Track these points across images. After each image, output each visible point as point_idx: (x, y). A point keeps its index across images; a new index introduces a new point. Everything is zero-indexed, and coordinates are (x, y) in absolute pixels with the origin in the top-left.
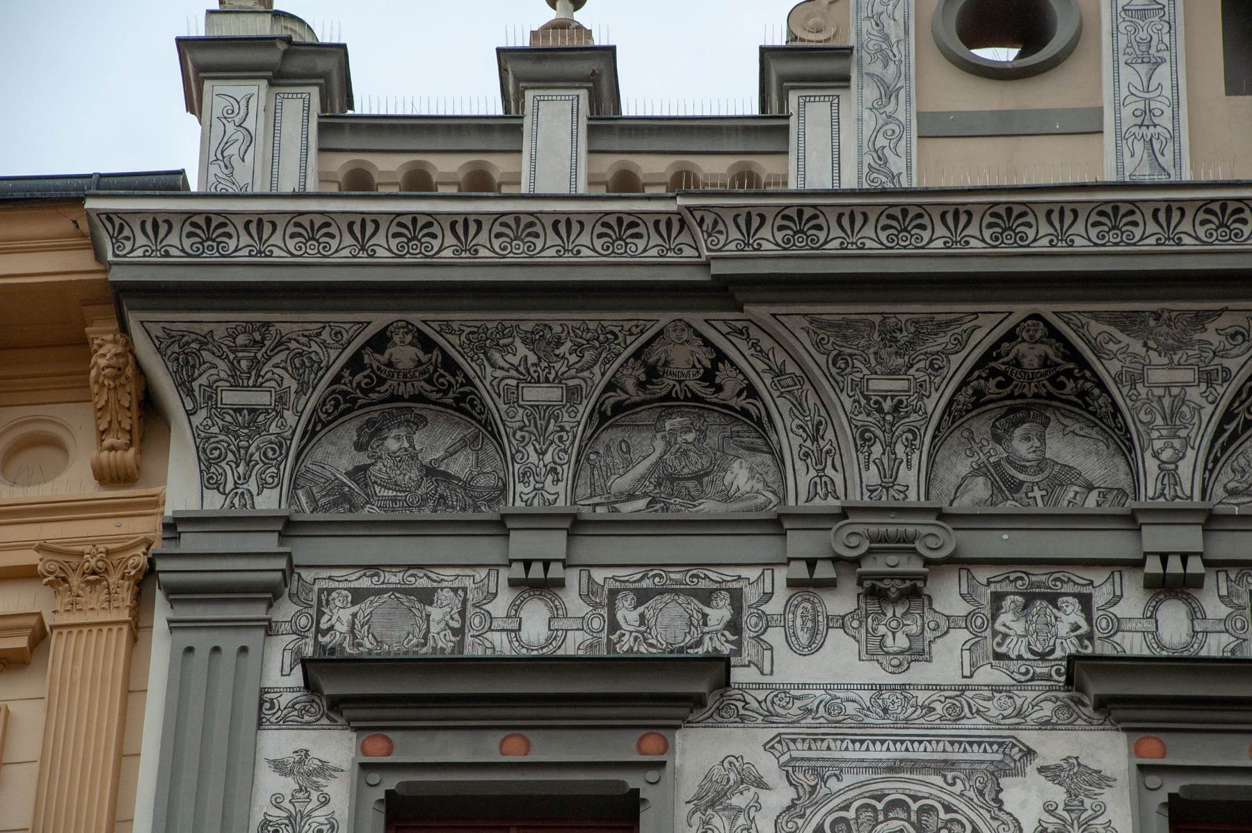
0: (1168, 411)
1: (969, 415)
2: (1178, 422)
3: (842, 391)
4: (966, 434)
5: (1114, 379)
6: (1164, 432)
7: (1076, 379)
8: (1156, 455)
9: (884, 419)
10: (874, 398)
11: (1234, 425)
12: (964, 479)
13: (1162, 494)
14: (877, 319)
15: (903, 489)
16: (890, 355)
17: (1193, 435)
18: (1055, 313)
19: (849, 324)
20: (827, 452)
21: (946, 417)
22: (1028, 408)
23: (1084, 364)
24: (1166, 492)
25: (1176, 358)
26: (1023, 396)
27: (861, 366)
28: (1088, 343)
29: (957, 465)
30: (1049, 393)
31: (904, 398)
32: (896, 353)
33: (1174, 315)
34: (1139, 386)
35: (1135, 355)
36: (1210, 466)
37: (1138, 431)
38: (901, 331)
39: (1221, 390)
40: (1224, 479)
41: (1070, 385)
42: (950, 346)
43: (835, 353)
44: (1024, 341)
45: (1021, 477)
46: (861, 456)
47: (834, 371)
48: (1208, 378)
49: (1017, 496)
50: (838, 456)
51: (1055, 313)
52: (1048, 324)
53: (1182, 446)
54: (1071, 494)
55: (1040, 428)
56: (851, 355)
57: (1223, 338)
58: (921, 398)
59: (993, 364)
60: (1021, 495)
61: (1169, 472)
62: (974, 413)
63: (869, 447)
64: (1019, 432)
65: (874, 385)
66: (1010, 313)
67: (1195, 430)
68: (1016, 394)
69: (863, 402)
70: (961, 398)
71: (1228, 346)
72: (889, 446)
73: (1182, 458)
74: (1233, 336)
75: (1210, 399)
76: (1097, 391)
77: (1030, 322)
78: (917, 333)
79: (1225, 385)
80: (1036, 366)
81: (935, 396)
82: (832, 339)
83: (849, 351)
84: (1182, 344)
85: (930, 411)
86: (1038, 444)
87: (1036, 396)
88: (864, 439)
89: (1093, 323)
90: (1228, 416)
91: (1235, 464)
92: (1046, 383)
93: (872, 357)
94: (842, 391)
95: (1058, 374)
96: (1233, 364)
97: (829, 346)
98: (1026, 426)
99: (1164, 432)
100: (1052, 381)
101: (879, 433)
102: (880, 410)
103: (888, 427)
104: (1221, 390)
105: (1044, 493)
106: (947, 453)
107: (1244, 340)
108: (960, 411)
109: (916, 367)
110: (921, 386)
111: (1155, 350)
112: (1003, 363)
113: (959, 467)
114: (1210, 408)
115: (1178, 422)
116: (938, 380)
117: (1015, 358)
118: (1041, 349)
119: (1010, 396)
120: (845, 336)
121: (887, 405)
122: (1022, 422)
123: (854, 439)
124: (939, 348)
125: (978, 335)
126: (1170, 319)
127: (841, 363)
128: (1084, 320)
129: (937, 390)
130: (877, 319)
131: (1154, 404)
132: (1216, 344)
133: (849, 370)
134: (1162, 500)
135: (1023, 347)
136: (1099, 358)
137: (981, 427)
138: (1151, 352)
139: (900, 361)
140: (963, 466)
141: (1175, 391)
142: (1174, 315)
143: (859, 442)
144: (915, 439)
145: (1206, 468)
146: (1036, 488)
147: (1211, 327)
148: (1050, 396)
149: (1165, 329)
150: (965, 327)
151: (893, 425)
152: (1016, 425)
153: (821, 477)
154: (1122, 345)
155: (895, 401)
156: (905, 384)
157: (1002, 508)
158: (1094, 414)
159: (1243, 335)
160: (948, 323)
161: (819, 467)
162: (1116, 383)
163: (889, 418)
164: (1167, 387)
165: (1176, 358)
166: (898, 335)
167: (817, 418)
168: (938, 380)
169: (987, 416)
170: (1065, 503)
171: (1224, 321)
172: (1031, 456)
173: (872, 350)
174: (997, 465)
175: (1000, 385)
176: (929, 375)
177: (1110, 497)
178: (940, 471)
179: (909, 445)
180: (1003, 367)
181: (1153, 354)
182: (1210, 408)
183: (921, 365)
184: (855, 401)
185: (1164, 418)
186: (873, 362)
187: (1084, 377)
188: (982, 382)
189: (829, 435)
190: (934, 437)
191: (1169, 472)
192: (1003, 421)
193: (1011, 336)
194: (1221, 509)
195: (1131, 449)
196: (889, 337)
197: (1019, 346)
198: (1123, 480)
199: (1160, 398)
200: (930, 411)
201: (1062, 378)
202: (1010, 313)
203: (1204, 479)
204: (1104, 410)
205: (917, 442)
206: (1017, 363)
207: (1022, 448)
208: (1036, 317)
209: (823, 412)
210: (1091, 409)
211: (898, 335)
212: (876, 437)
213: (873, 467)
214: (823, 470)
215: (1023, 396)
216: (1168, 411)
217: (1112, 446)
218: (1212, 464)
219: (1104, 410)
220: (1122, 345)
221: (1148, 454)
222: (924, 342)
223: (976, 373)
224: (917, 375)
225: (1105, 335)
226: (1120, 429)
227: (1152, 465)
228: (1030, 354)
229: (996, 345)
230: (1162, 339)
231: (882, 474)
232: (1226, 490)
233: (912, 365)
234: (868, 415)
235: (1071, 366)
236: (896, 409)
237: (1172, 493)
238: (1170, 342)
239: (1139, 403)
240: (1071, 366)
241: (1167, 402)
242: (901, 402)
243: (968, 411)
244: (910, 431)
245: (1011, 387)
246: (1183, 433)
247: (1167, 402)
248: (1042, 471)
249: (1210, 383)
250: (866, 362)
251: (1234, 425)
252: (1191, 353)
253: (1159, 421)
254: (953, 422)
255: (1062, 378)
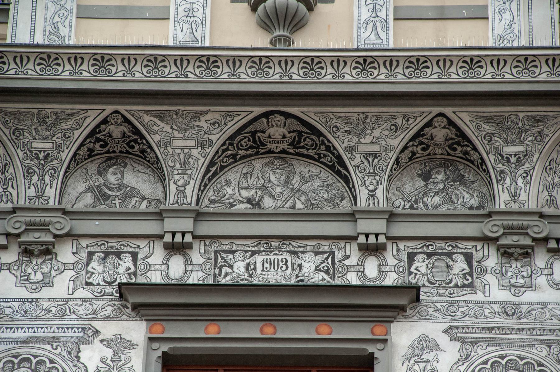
0: (182, 161)
1: (87, 161)
2: (187, 167)
3: (18, 148)
4: (84, 171)
5: (156, 144)
6: (180, 171)
7: (139, 144)
8: (175, 183)
9: (40, 163)
10: (35, 152)
11: (215, 168)
12: (81, 193)
13: (177, 202)
14: (36, 111)
15: (47, 198)
16: (43, 130)
17: (194, 173)
18: (126, 110)
19: (21, 113)
20: (9, 179)
21: (73, 162)
22: (117, 158)
23: (142, 137)
24: (179, 201)
25: (186, 134)
26: (114, 152)
27: (28, 135)
28: (143, 126)
29: (77, 186)
30: (127, 151)
31: (50, 152)
32: (46, 129)
33: (185, 112)
34: (169, 148)
35: (166, 132)
36: (202, 188)
37: (167, 170)
38: (48, 117)
39: (208, 151)
40: (209, 195)
41: (137, 147)
42: (74, 126)
43: (14, 128)
44: (112, 124)
45: (110, 193)
46: (26, 181)
47: (13, 137)
48: (202, 145)
49: (106, 203)
50: (15, 181)
51: (126, 110)
52: (123, 116)
53: (188, 179)
54: (134, 202)
55: (121, 168)
56: (22, 130)
57: (209, 125)
58: (59, 152)
59: (97, 136)
60: (109, 202)
61: (181, 191)
62: (89, 160)
63: (31, 177)
64: (111, 170)
65: (35, 145)
66: (104, 110)
67: (195, 171)
68: (111, 151)
69: (29, 154)
70: (81, 153)
71: (212, 129)
72: (42, 176)
73: (188, 184)
74: (214, 124)
75: (203, 155)
76: (149, 150)
77: (114, 115)
78: (57, 118)
79: (210, 148)
80: (120, 137)
81: (66, 151)
82: (12, 121)
83: (21, 127)
84: (189, 127)
85: (63, 159)
86: (120, 176)
87: (121, 152)
88: (29, 173)
89: (145, 116)
90: (212, 163)
91: (215, 188)
92: (125, 145)
93: (33, 131)
94: (18, 148)
95: (130, 141)
96: (214, 138)
97: (11, 125)
98: (115, 167)
99: (180, 171)
100: (128, 144)
101: (36, 170)
102: (38, 158)
103: (41, 166)
104: (208, 151)
105: (120, 201)
106: (73, 180)
107: (219, 126)
108: (81, 159)
109: (56, 136)
110: (59, 146)
111: (176, 130)
112: (102, 135)
113: (79, 188)
114: (202, 160)
115: (187, 167)
116: (68, 143)
117: (109, 133)
118: (121, 128)
119: (108, 152)
120: (19, 120)
121: (41, 156)
122: (113, 165)
123: (23, 173)
124: (69, 127)
125: (88, 121)
126: (183, 115)
127: (17, 134)
128: (141, 114)
129: (67, 148)
130: (36, 111)
131: (176, 157)
132: (206, 128)
133: (21, 137)
134: (176, 205)
135: (112, 127)
136: (149, 134)
137: (92, 167)
138: (174, 131)
139: (48, 133)
140: (81, 187)
141: (186, 151)
142: (185, 112)
143: (26, 174)
144: (55, 173)
145: (199, 189)
146: (117, 199)
147: (203, 119)
148: (127, 152)
149: (181, 120)
150: (81, 116)
151: (44, 166)
152: (110, 167)
153: (5, 192)
154: (160, 127)
155: (46, 153)
156: (50, 145)
157: (97, 209)
158: (148, 161)
159: (218, 123)
160: (73, 114)
161: (5, 187)
162: (157, 146)
163: (42, 162)
164: (182, 149)
165: (186, 134)
166: (47, 120)
167: (5, 162)
168: (68, 143)
169: (96, 162)
170: (130, 206)
171: (209, 117)
172: (116, 182)
173: (33, 127)
174: (98, 187)
175: (101, 146)
176: (63, 140)
177: (153, 203)
178: (69, 190)
179: (52, 176)
180: (103, 137)
181: (175, 132)
182: (202, 160)
183: (59, 135)
184: (24, 153)
185: (180, 164)
186: (34, 134)
187: (142, 143)
188: (92, 144)
189: (11, 170)
190: (66, 172)
191: (181, 191)
192: (104, 164)
193: (105, 121)
194: (206, 210)
195: (165, 180)
196: (42, 120)
197: (110, 127)
198: (160, 195)
199: (179, 154)
200: (63, 159)
201: (132, 143)
202: (104, 110)
203: (198, 195)
204: (153, 160)
205: (56, 175)
206: (110, 136)
207: (112, 178)
208: (117, 112)
209: (8, 159)
210: (147, 159)
211: (47, 120)
212: (35, 172)
213: (32, 187)
214: (7, 188)
215: (114, 152)
216: (182, 161)
217: (157, 178)
218: (203, 187)
219: (153, 160)
220: (160, 127)
221: (172, 182)
222: (61, 123)
223: (88, 140)
224: (57, 140)
225: (152, 122)
226: (160, 170)
227: (173, 187)
228: (117, 130)
229: (98, 126)
230: (179, 125)
231: (37, 191)
232: (209, 200)
233: (55, 135)
234: (31, 160)
235: (136, 137)
236: (46, 157)
237: (182, 201)
238: (184, 126)
239: (168, 157)
240: (136, 137)
241: (182, 156)
242: (48, 154)
243: (85, 159)
244: (53, 169)
245: (108, 147)
246: (189, 172)
247: (182, 156)
248: (121, 190)
249: (203, 148)
250: (30, 133)
251: (215, 168)
252: (194, 132)
253: (178, 166)
254: (77, 165)
255: (132, 143)
